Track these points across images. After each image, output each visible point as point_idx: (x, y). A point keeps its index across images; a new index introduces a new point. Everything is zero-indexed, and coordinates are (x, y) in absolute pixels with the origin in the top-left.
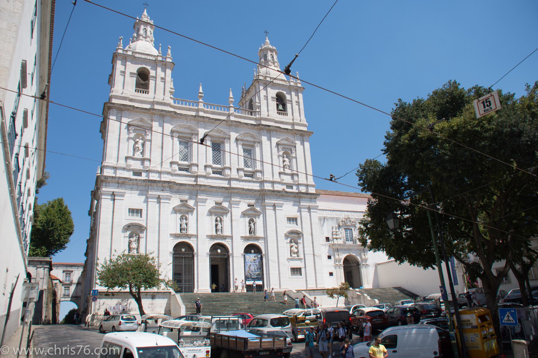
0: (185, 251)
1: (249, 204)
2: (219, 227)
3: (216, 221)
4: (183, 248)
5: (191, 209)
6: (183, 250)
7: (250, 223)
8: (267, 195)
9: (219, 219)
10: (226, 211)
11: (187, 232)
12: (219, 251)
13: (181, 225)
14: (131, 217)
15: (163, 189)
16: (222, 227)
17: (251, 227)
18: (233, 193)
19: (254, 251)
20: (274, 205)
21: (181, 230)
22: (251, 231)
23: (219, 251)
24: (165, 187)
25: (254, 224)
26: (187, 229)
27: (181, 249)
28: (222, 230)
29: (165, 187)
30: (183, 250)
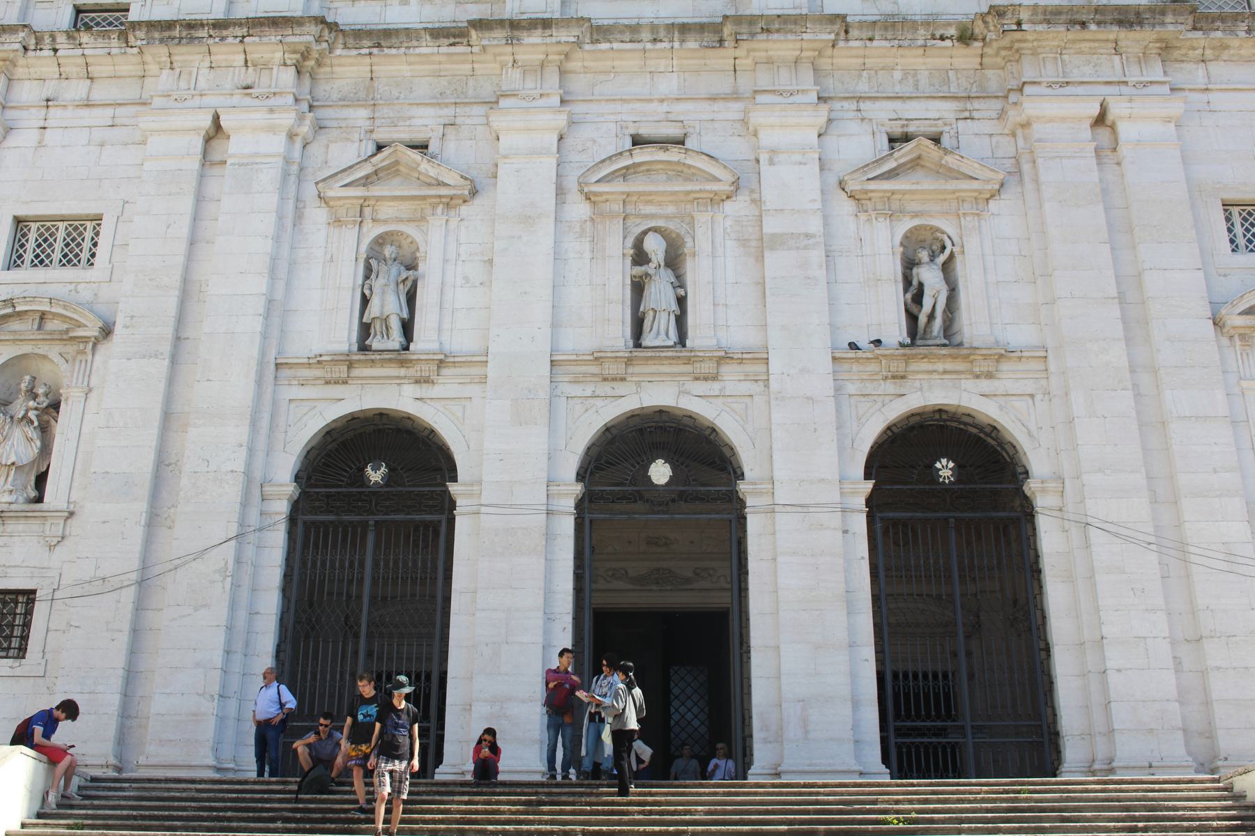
0: (389, 480)
1: (897, 130)
2: (660, 294)
3: (640, 257)
4: (375, 457)
5: (443, 191)
6: (376, 475)
7: (910, 264)
8: (1035, 53)
9: (656, 246)
10: (715, 187)
11: (407, 348)
12: (660, 472)
13: (365, 301)
14: (26, 274)
15: (249, 82)
16: (681, 301)
17: (921, 285)
18: (769, 61)
19: (959, 468)
20: (1100, 120)
21: (365, 330)
22: (923, 319)
23: (660, 472)
24: (266, 66)
25: (947, 267)
26: (407, 328)
27: (362, 470)
28: (681, 321)
29: (266, 66)
30: (376, 475)
